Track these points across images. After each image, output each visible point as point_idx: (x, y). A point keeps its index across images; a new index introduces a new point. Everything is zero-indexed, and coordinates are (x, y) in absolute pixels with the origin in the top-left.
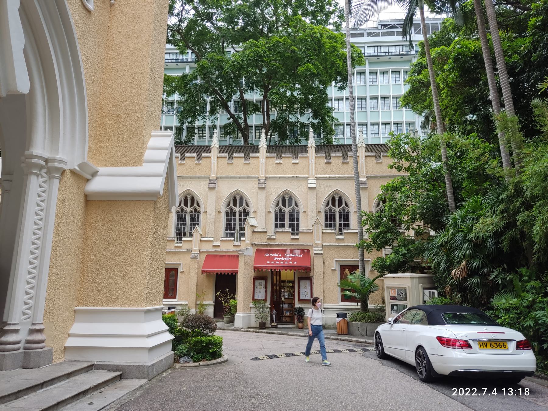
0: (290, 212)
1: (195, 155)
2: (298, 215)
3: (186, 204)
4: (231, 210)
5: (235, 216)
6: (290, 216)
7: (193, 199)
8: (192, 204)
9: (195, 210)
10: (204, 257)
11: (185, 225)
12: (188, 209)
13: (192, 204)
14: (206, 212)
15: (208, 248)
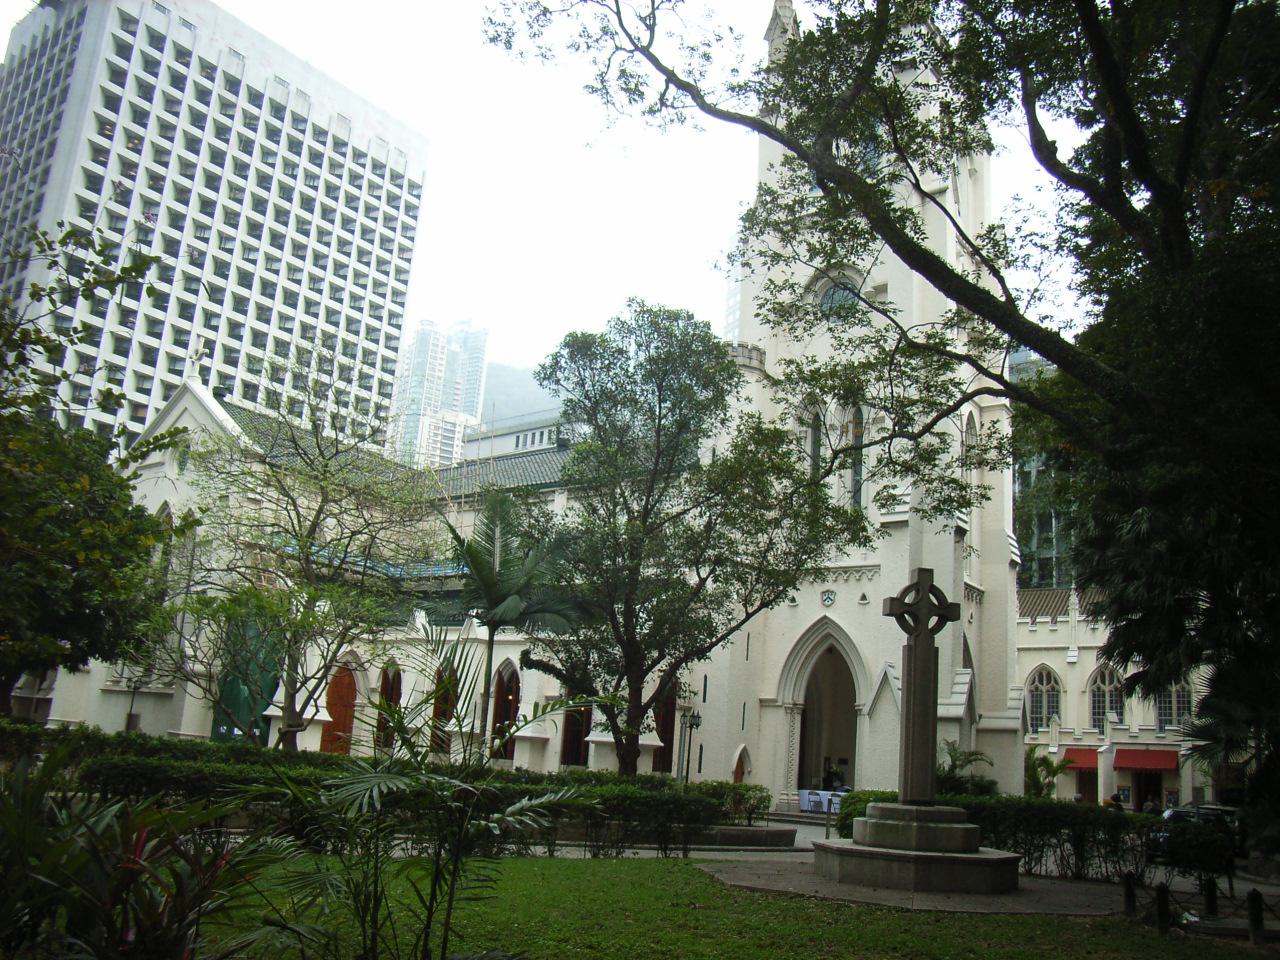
0: (1177, 691)
1: (1049, 619)
2: (1189, 696)
3: (1041, 682)
4: (1099, 688)
5: (1104, 696)
6: (1178, 696)
7: (1049, 675)
8: (1049, 682)
9: (1053, 689)
10: (1064, 750)
11: (1041, 707)
12: (1044, 688)
13: (1049, 682)
14: (1065, 692)
15: (1068, 741)
